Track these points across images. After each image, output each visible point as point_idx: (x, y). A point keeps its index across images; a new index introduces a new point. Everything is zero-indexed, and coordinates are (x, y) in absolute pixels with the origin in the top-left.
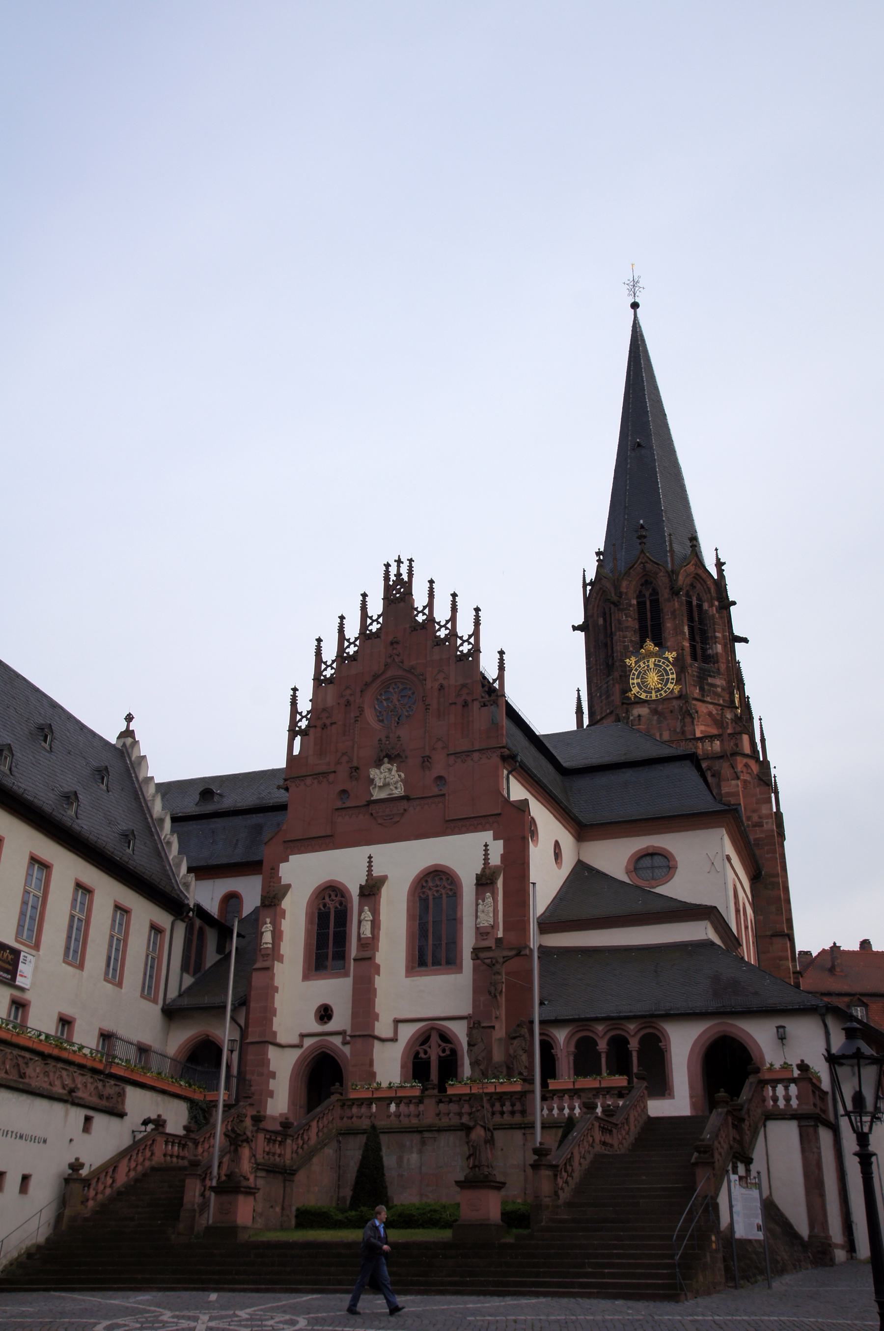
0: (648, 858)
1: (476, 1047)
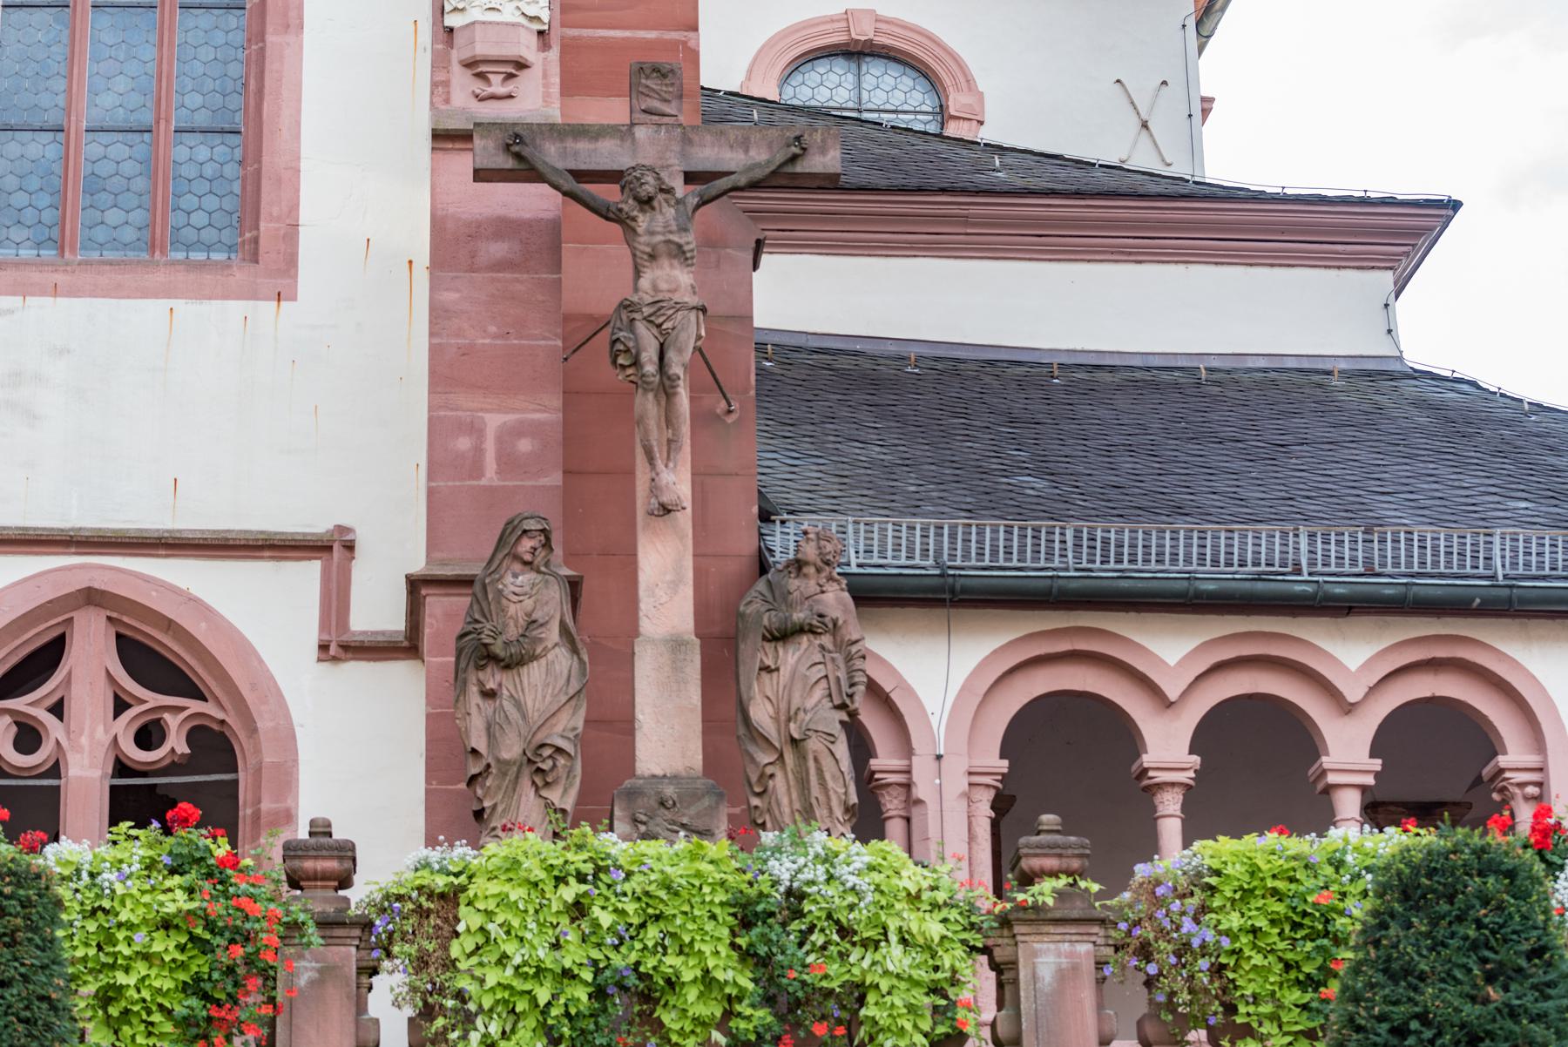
0: (840, 65)
1: (533, 673)
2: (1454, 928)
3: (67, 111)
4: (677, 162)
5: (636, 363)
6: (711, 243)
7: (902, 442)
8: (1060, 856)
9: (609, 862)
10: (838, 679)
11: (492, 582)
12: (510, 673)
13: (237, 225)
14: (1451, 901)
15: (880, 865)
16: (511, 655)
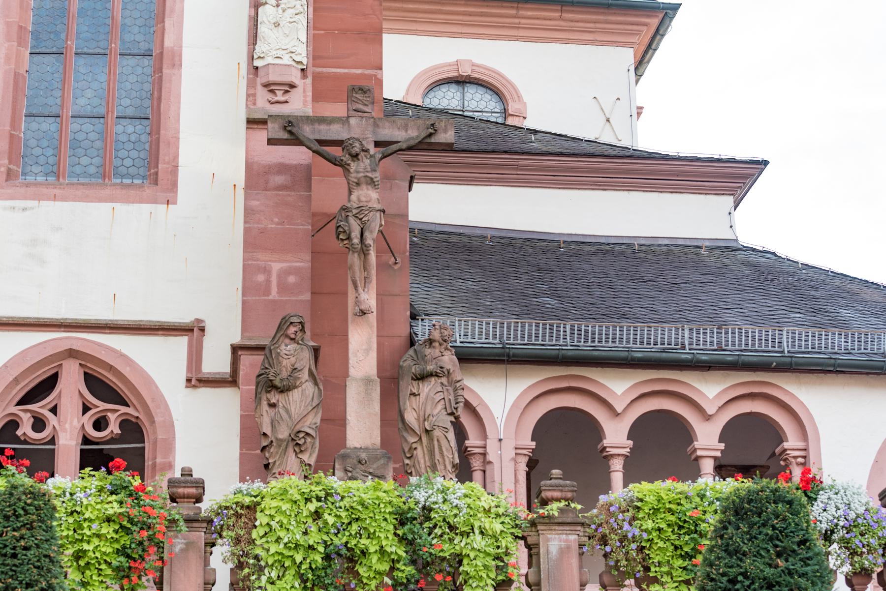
0: (453, 88)
1: (295, 395)
2: (761, 529)
3: (62, 106)
4: (371, 136)
5: (349, 238)
6: (387, 177)
7: (484, 280)
8: (562, 491)
9: (333, 491)
10: (450, 400)
11: (274, 348)
12: (283, 395)
13: (147, 166)
14: (759, 515)
15: (470, 494)
16: (284, 386)
